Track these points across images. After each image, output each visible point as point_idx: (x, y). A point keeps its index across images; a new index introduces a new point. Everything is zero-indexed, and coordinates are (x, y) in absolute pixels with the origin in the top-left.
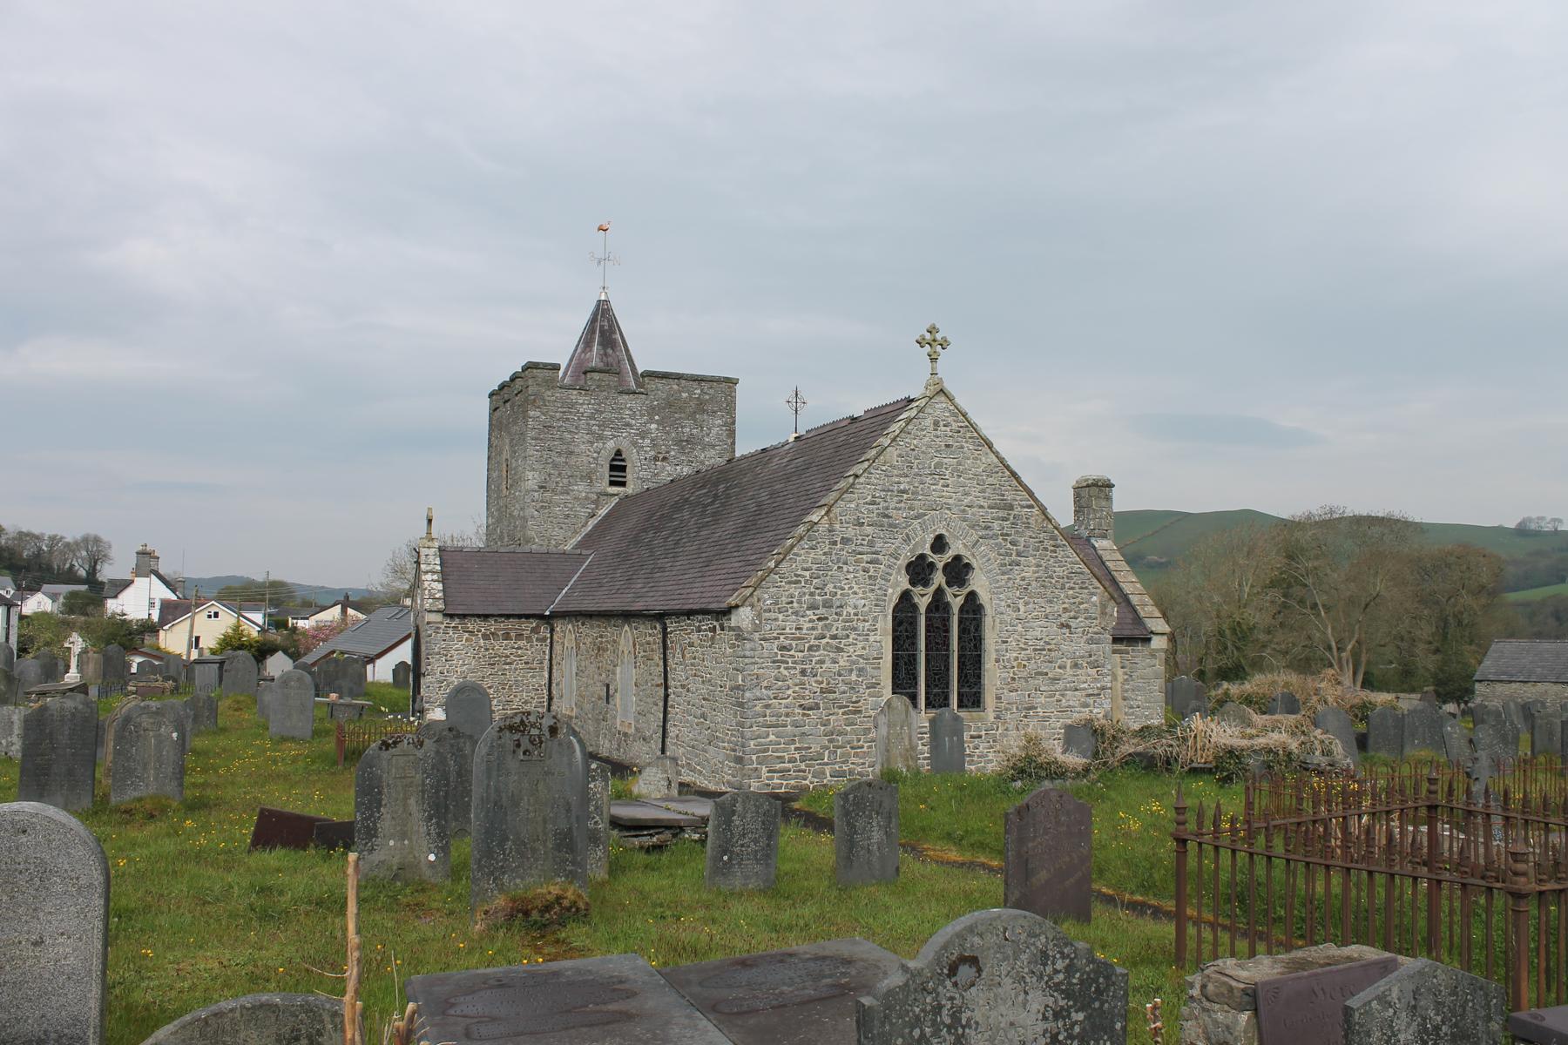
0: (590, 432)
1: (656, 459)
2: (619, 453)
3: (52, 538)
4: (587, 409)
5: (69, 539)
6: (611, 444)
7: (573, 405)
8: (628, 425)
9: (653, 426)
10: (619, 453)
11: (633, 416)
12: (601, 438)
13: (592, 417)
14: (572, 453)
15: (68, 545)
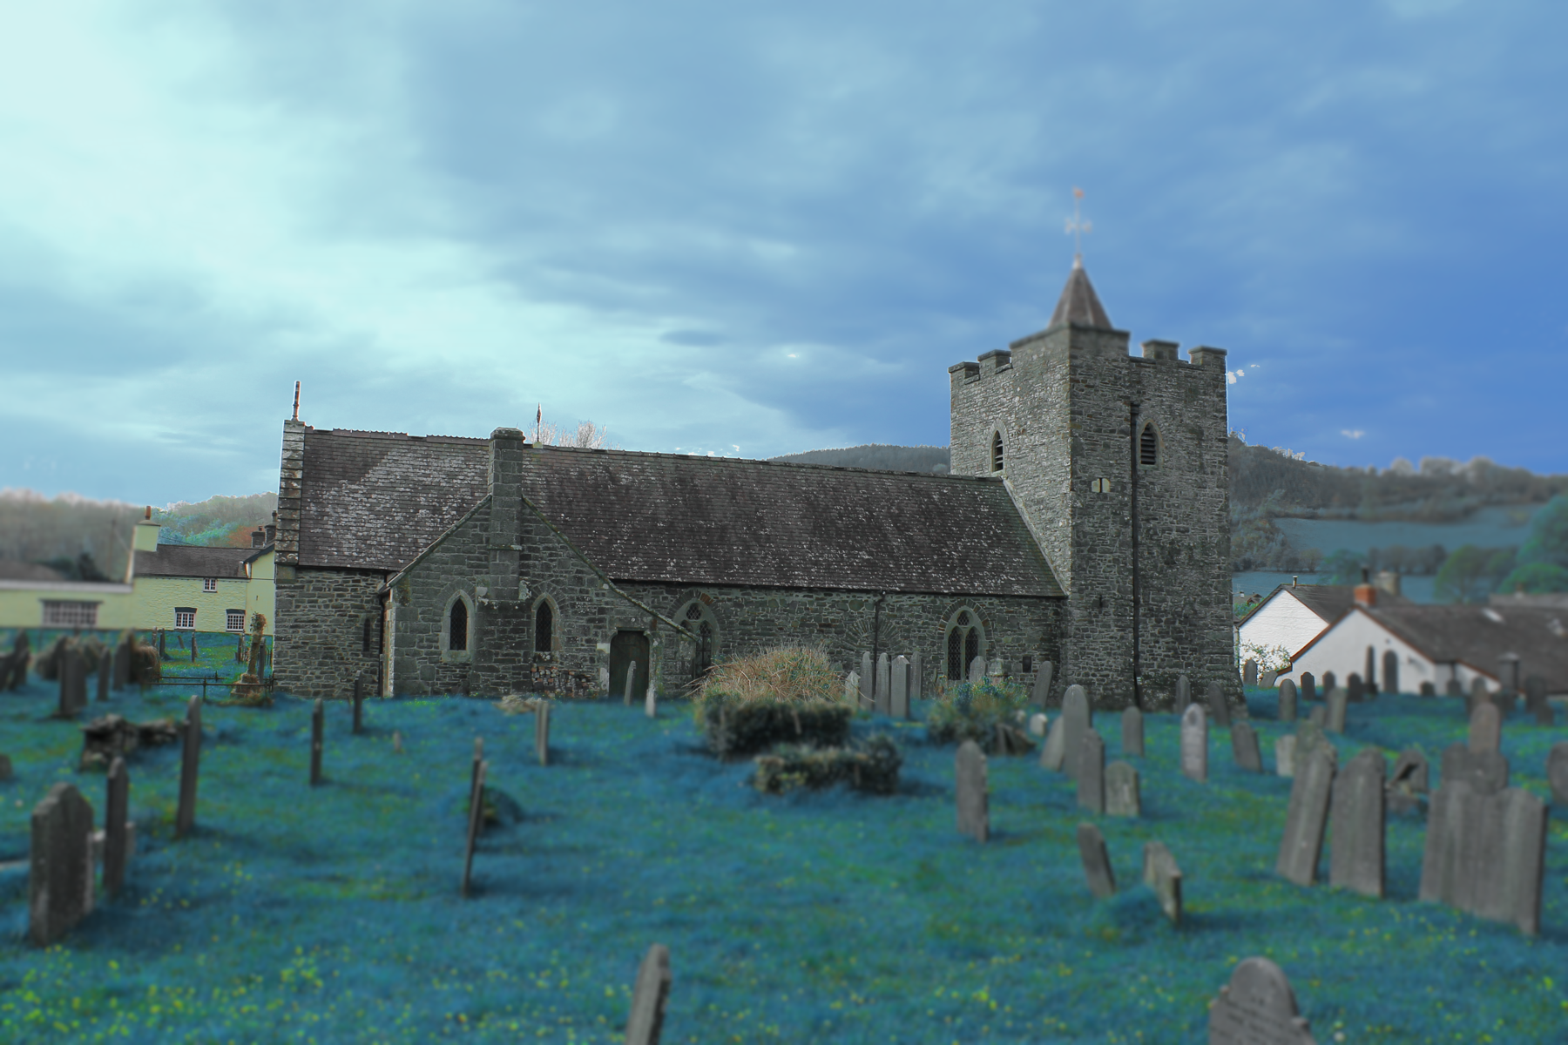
2: (998, 435)
4: (979, 399)
6: (993, 428)
10: (998, 435)
14: (972, 445)
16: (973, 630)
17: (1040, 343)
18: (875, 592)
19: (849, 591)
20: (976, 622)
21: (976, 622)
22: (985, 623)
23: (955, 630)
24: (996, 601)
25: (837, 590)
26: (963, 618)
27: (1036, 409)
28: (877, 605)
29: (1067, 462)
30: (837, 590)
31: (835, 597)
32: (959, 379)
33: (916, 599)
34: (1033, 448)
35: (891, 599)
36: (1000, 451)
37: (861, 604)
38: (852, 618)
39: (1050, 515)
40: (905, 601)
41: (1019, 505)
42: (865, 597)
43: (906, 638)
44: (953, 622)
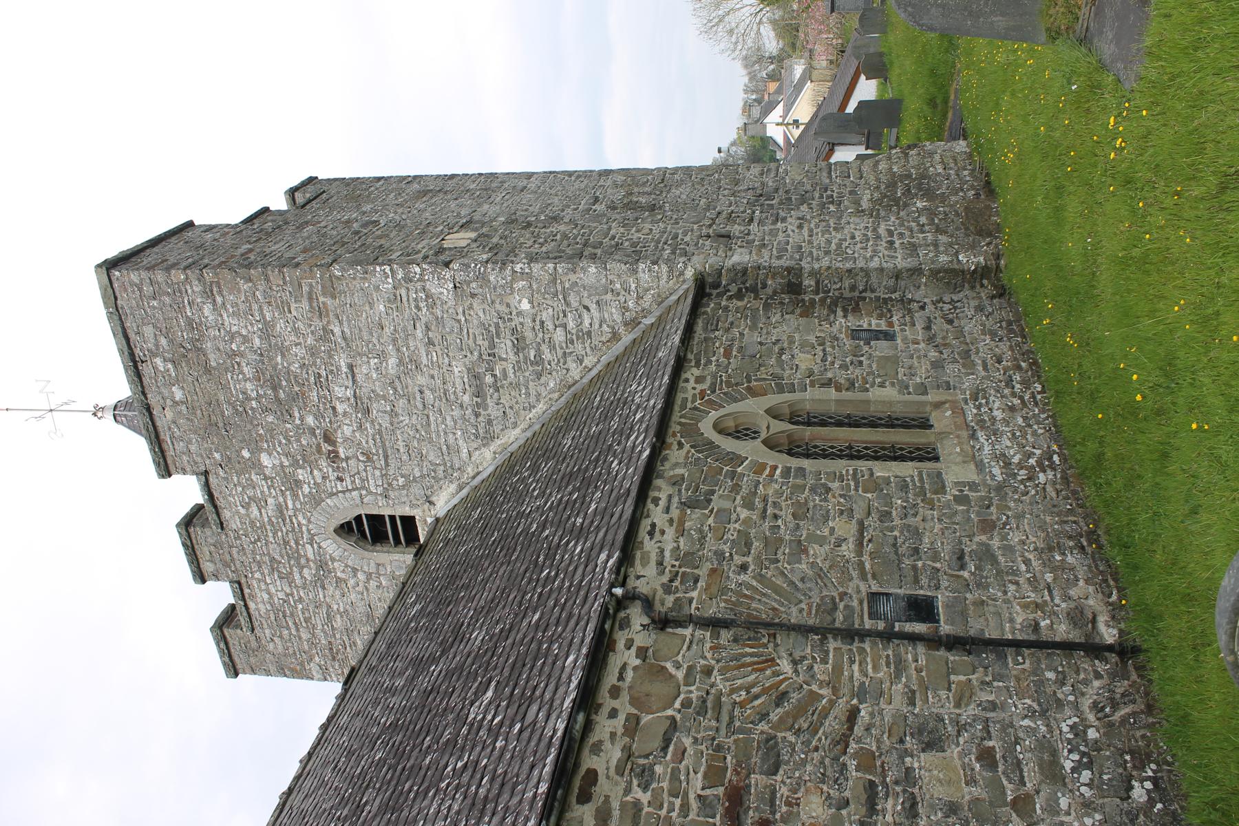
0: (319, 582)
1: (333, 457)
2: (345, 529)
3: (746, 91)
4: (279, 589)
5: (746, 79)
6: (333, 547)
7: (276, 611)
8: (280, 509)
9: (265, 460)
10: (345, 529)
11: (261, 503)
12: (322, 565)
13: (288, 578)
15: (751, 79)
16: (773, 413)
17: (146, 370)
18: (613, 613)
19: (587, 699)
20: (753, 408)
21: (753, 408)
22: (752, 392)
23: (770, 444)
24: (692, 373)
25: (572, 747)
26: (742, 432)
27: (284, 394)
28: (662, 623)
29: (383, 279)
30: (572, 747)
31: (604, 759)
32: (247, 650)
33: (657, 514)
34: (362, 406)
35: (646, 578)
36: (376, 521)
37: (652, 668)
38: (708, 706)
39: (505, 347)
40: (663, 539)
41: (487, 460)
42: (624, 657)
43: (800, 549)
44: (750, 450)
